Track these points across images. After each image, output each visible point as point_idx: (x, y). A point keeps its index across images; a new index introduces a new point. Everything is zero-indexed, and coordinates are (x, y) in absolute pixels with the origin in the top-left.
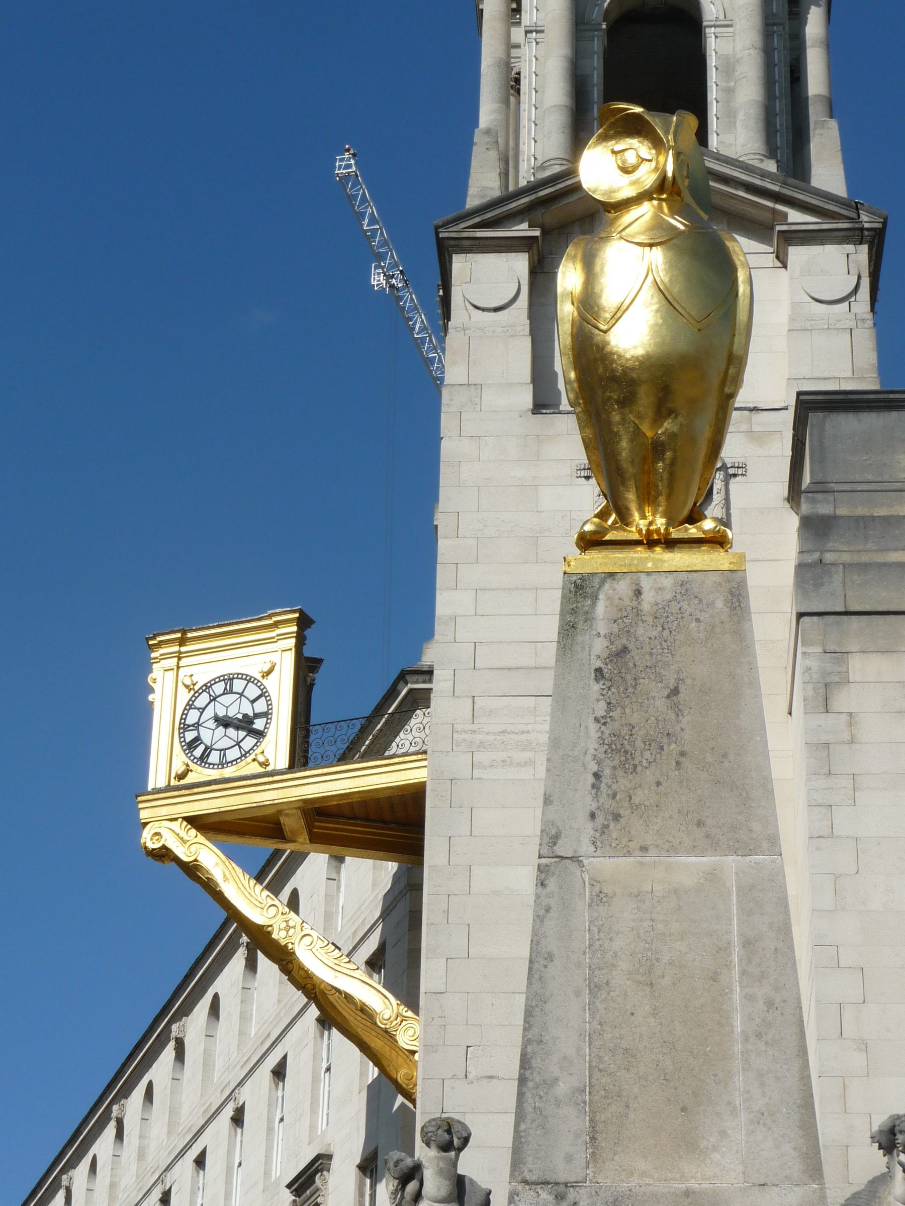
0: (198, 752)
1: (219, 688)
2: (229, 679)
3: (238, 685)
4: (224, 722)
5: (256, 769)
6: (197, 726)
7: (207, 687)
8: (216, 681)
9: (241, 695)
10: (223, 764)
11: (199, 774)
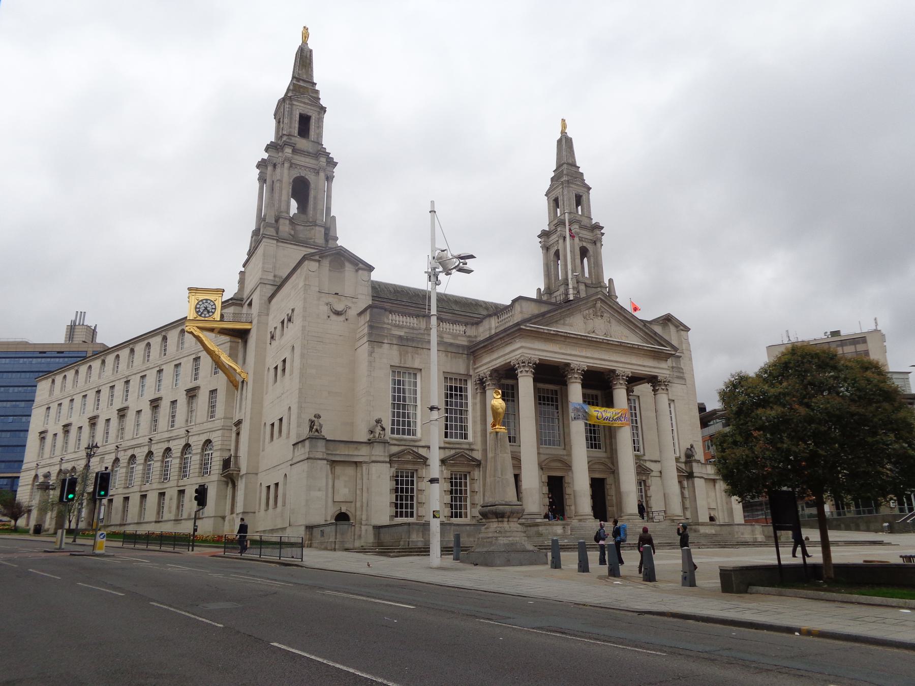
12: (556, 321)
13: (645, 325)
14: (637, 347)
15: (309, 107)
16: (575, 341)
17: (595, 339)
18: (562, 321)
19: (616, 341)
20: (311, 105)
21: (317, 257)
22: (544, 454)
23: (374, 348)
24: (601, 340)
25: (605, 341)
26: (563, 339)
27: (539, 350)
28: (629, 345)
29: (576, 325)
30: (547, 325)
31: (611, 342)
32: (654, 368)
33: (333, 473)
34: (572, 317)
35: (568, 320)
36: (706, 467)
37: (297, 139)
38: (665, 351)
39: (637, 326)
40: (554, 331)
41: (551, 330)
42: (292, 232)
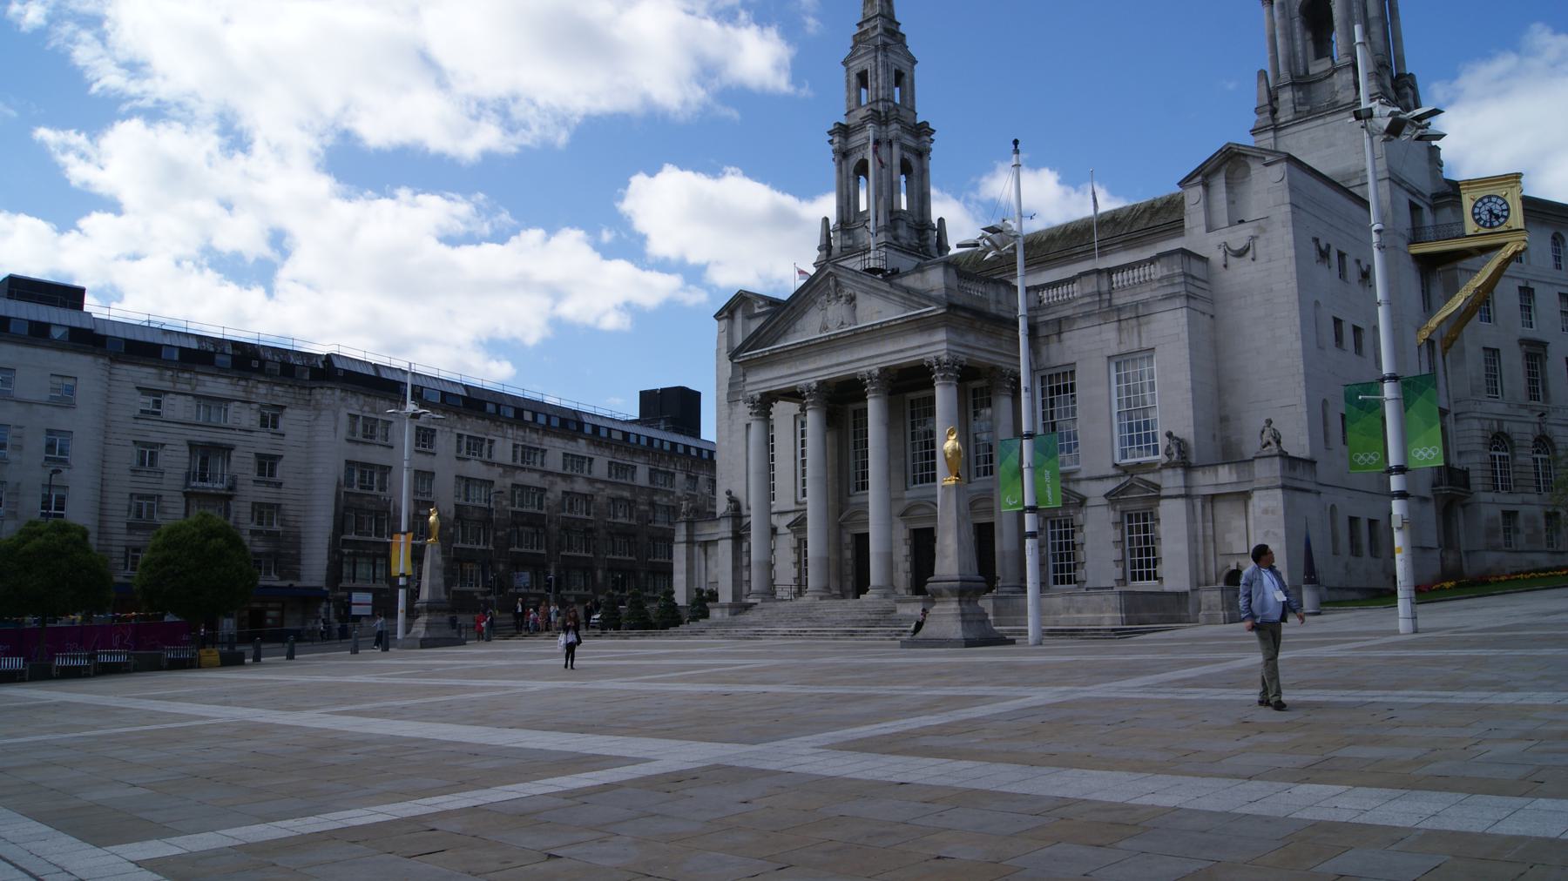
0: (1482, 223)
1: (1486, 200)
2: (1489, 197)
3: (1494, 199)
4: (1490, 211)
5: (1506, 229)
6: (1479, 214)
7: (1481, 200)
8: (1485, 197)
9: (1495, 203)
10: (1491, 227)
11: (1483, 231)
12: (785, 332)
13: (891, 286)
14: (878, 326)
15: (865, 58)
16: (801, 351)
17: (819, 341)
18: (792, 328)
19: (848, 331)
20: (865, 54)
21: (726, 314)
22: (909, 499)
23: (732, 409)
24: (827, 339)
25: (832, 338)
26: (786, 355)
27: (762, 382)
28: (868, 329)
29: (809, 328)
30: (773, 343)
31: (842, 335)
32: (920, 347)
33: (706, 554)
34: (804, 317)
35: (799, 325)
36: (1217, 471)
37: (855, 113)
38: (926, 315)
39: (887, 292)
40: (769, 351)
41: (765, 352)
42: (850, 242)
